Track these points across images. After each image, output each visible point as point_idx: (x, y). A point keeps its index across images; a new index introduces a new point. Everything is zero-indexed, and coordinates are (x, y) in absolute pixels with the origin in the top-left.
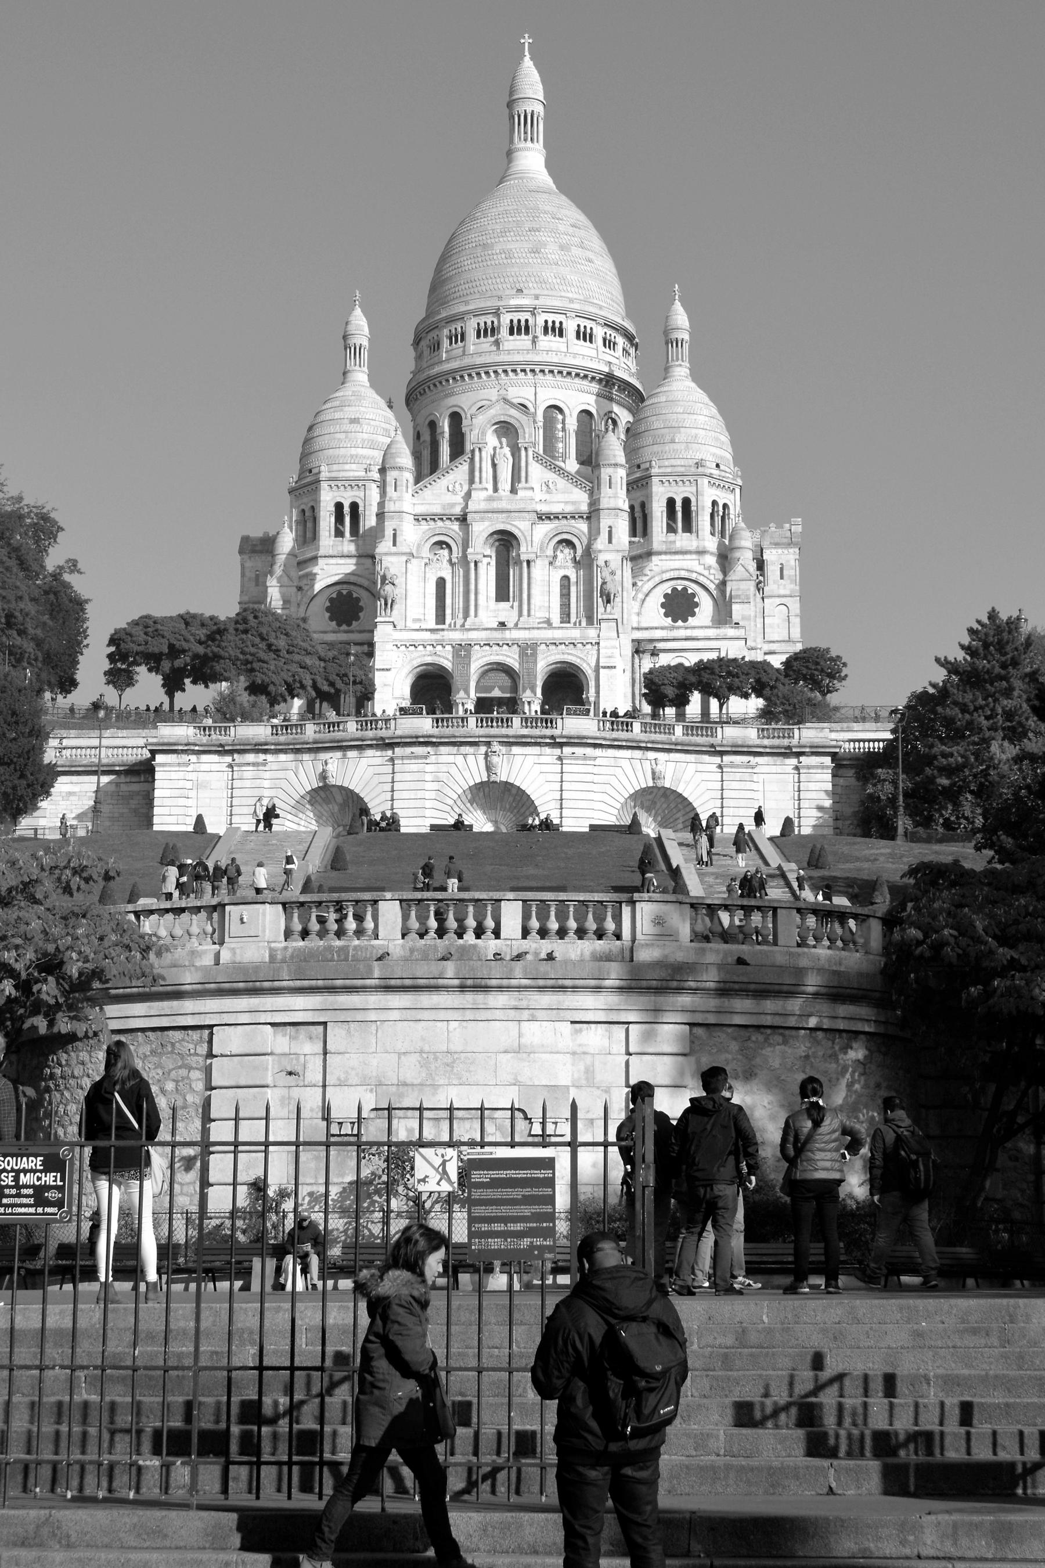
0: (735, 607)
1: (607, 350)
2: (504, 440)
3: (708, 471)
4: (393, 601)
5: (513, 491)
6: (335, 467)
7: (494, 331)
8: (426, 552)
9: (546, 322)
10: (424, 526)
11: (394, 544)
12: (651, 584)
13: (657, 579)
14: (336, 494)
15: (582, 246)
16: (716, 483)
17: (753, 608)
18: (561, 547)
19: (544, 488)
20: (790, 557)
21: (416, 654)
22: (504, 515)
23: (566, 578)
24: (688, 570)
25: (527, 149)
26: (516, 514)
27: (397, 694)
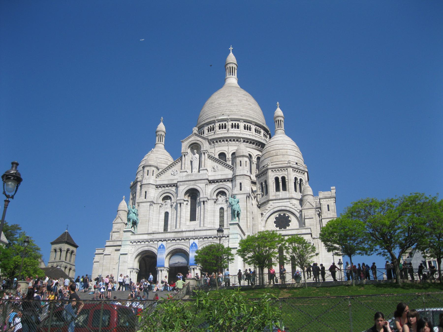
0: (306, 220)
1: (257, 134)
3: (292, 166)
5: (199, 172)
7: (213, 129)
8: (160, 201)
9: (232, 124)
10: (160, 190)
11: (145, 198)
12: (269, 214)
13: (272, 211)
15: (247, 100)
16: (296, 169)
17: (315, 221)
19: (213, 170)
20: (332, 202)
21: (141, 246)
23: (222, 209)
24: (285, 206)
25: (230, 77)
26: (199, 181)
27: (131, 266)
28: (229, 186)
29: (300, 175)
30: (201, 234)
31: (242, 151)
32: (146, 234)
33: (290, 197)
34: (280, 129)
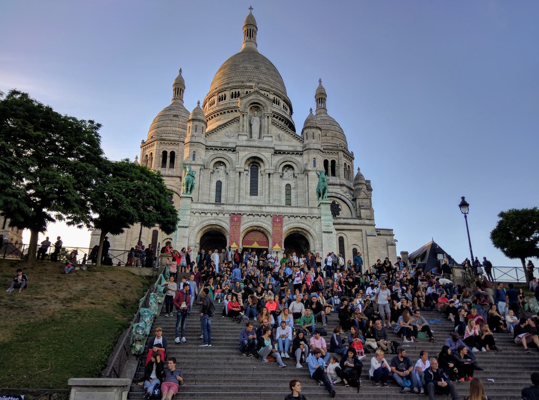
0: (362, 211)
2: (256, 112)
4: (192, 186)
6: (164, 135)
8: (211, 166)
10: (211, 153)
11: (194, 159)
14: (164, 147)
18: (286, 169)
19: (277, 138)
21: (206, 219)
22: (257, 149)
23: (288, 185)
25: (251, 42)
26: (263, 149)
27: (192, 242)
28: (298, 160)
29: (348, 162)
30: (285, 211)
31: (315, 122)
32: (213, 204)
33: (341, 183)
34: (323, 108)
